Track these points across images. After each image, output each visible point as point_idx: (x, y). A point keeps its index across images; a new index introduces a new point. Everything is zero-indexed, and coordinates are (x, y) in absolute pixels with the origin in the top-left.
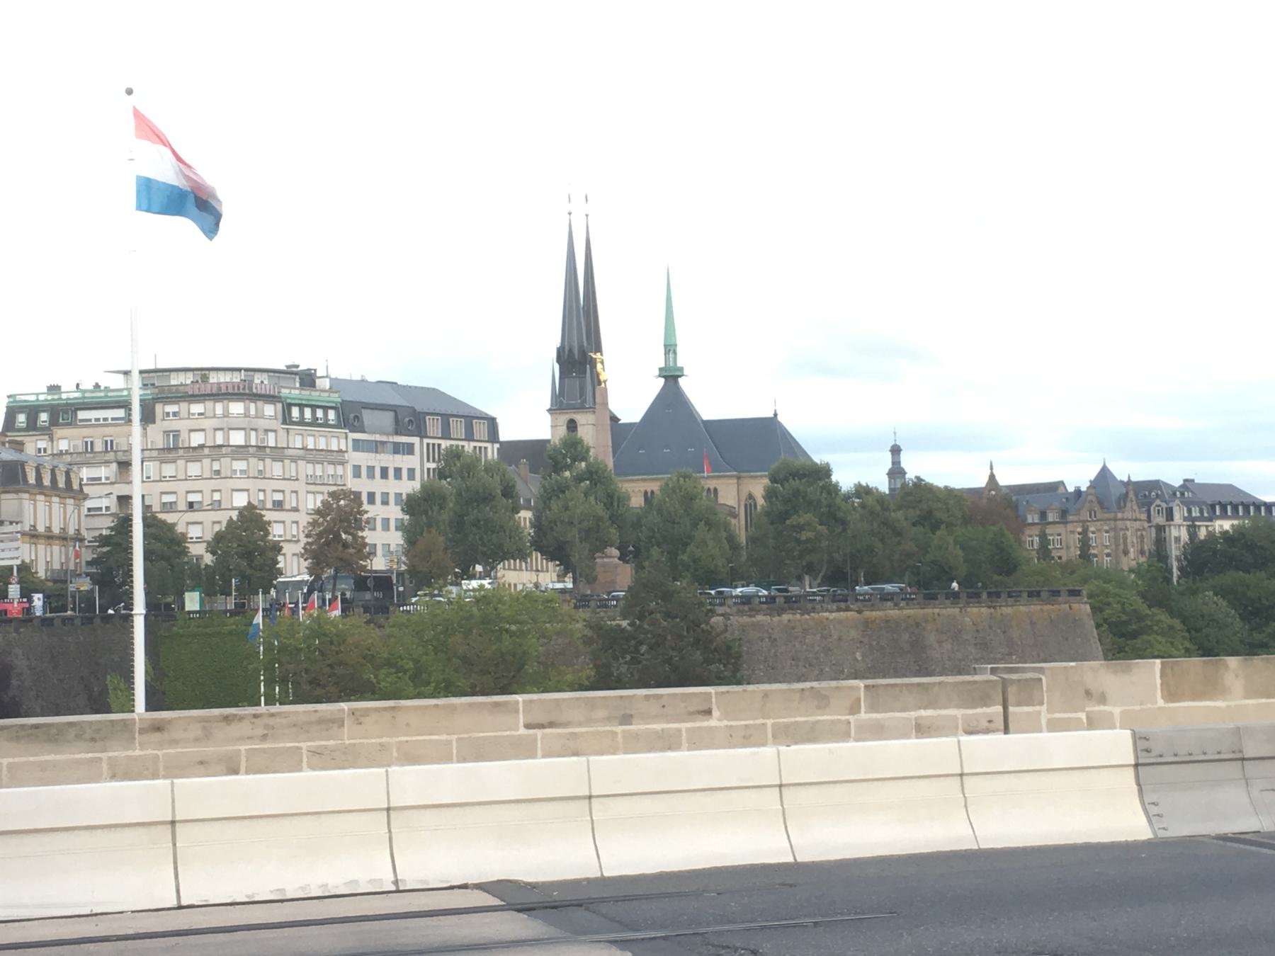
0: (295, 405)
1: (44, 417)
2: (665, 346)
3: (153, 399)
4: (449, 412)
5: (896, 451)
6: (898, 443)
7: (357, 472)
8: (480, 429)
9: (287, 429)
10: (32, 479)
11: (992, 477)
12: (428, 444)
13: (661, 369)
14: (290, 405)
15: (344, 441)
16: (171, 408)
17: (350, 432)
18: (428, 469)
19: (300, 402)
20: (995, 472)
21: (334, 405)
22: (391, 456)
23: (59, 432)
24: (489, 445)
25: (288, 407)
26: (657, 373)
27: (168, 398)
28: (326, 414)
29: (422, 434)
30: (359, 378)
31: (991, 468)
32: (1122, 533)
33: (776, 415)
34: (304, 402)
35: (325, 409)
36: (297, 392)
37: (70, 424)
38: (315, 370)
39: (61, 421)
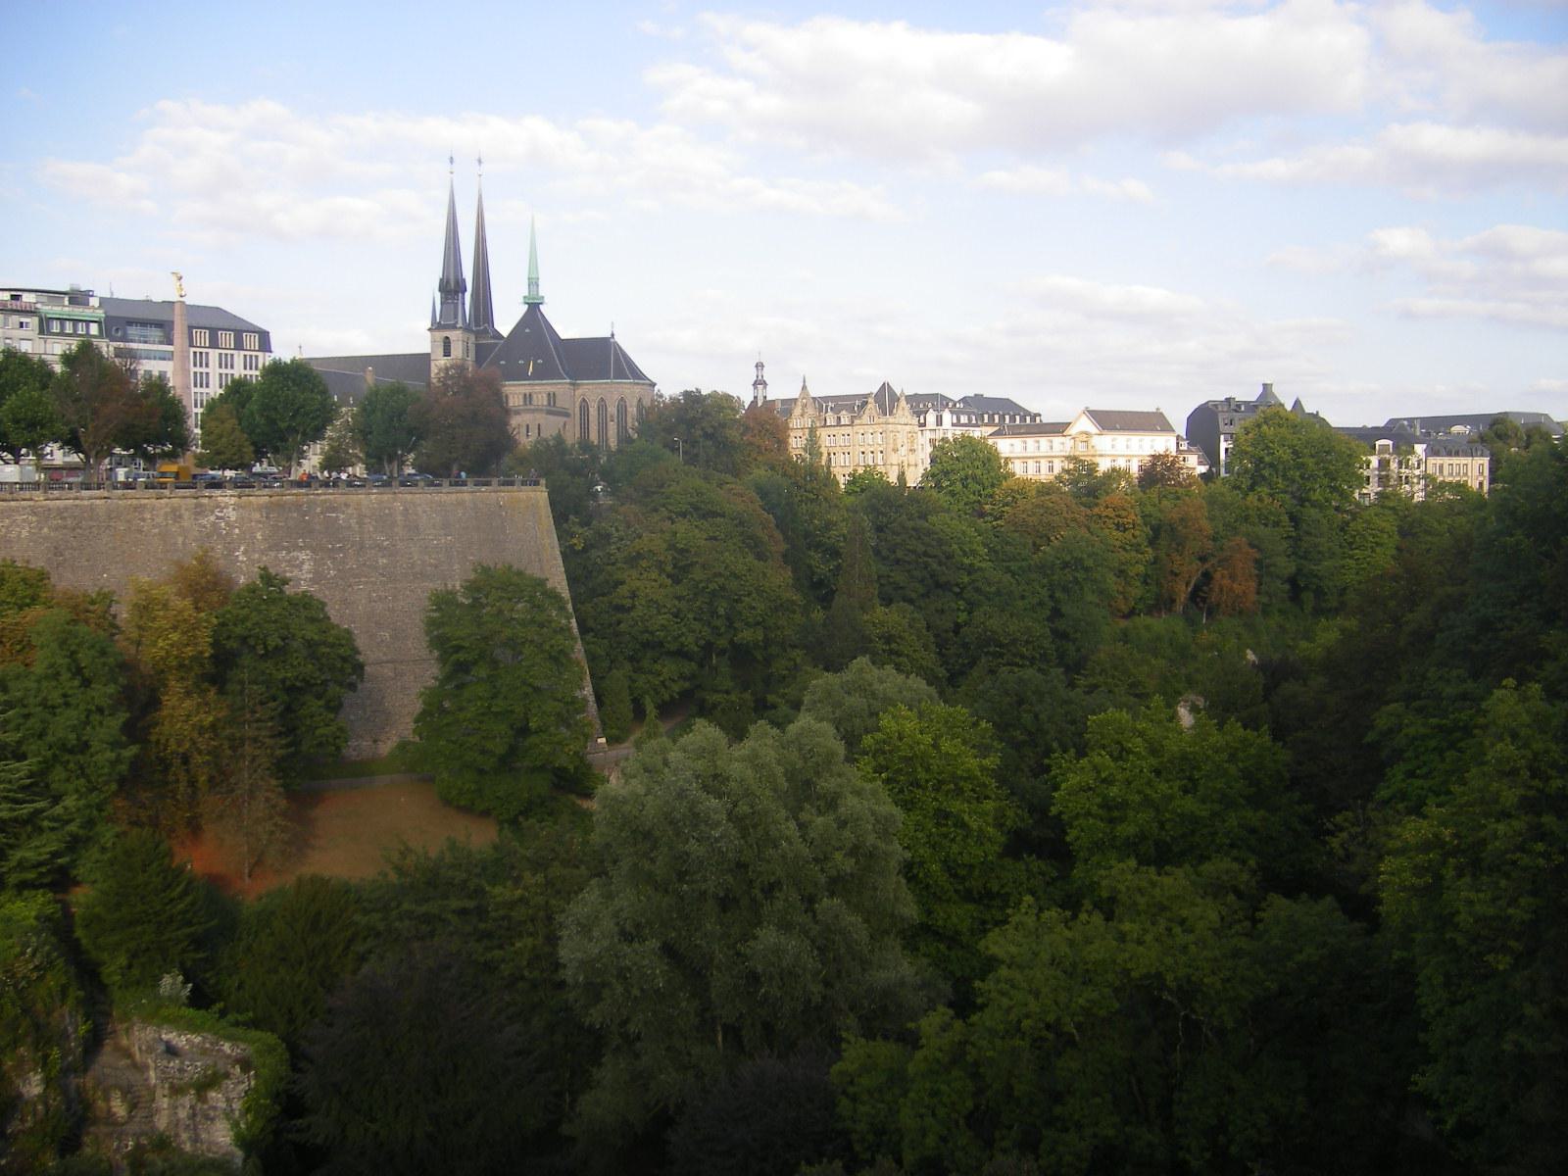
2: (529, 279)
4: (221, 325)
5: (760, 366)
8: (251, 341)
11: (804, 388)
12: (195, 353)
13: (525, 297)
18: (195, 373)
24: (260, 354)
26: (522, 300)
30: (144, 298)
31: (804, 382)
32: (892, 435)
33: (613, 335)
34: (65, 317)
36: (67, 309)
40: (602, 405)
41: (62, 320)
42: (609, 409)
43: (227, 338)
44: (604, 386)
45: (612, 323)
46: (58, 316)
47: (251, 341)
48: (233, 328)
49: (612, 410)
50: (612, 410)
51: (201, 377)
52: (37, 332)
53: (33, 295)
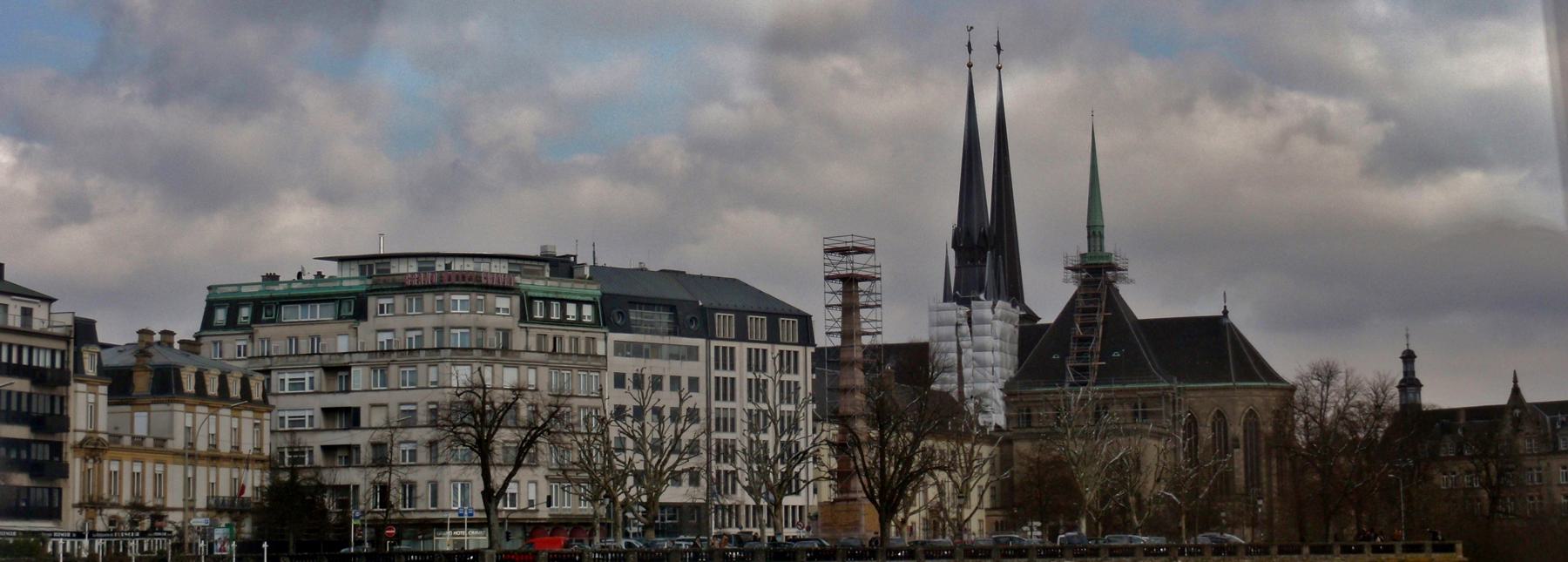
0: (588, 302)
1: (245, 312)
2: (1089, 227)
3: (367, 291)
6: (1411, 348)
7: (619, 381)
8: (788, 328)
9: (526, 328)
10: (189, 386)
11: (1516, 391)
12: (717, 348)
14: (531, 299)
15: (604, 343)
16: (385, 301)
17: (611, 331)
18: (717, 379)
19: (545, 295)
20: (1520, 384)
21: (591, 299)
22: (667, 362)
23: (263, 331)
24: (800, 349)
25: (527, 303)
27: (383, 290)
28: (579, 310)
29: (708, 333)
30: (637, 266)
31: (1515, 381)
33: (1225, 312)
34: (551, 296)
35: (579, 304)
37: (273, 321)
38: (575, 257)
39: (264, 317)
40: (1220, 419)
41: (547, 301)
42: (1231, 429)
43: (758, 325)
44: (1222, 393)
45: (1225, 293)
46: (541, 295)
47: (788, 328)
48: (763, 309)
49: (1236, 430)
50: (1236, 430)
51: (725, 384)
52: (518, 319)
53: (505, 263)
